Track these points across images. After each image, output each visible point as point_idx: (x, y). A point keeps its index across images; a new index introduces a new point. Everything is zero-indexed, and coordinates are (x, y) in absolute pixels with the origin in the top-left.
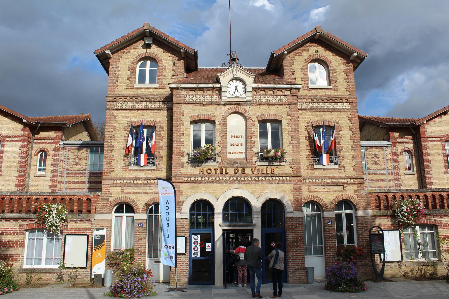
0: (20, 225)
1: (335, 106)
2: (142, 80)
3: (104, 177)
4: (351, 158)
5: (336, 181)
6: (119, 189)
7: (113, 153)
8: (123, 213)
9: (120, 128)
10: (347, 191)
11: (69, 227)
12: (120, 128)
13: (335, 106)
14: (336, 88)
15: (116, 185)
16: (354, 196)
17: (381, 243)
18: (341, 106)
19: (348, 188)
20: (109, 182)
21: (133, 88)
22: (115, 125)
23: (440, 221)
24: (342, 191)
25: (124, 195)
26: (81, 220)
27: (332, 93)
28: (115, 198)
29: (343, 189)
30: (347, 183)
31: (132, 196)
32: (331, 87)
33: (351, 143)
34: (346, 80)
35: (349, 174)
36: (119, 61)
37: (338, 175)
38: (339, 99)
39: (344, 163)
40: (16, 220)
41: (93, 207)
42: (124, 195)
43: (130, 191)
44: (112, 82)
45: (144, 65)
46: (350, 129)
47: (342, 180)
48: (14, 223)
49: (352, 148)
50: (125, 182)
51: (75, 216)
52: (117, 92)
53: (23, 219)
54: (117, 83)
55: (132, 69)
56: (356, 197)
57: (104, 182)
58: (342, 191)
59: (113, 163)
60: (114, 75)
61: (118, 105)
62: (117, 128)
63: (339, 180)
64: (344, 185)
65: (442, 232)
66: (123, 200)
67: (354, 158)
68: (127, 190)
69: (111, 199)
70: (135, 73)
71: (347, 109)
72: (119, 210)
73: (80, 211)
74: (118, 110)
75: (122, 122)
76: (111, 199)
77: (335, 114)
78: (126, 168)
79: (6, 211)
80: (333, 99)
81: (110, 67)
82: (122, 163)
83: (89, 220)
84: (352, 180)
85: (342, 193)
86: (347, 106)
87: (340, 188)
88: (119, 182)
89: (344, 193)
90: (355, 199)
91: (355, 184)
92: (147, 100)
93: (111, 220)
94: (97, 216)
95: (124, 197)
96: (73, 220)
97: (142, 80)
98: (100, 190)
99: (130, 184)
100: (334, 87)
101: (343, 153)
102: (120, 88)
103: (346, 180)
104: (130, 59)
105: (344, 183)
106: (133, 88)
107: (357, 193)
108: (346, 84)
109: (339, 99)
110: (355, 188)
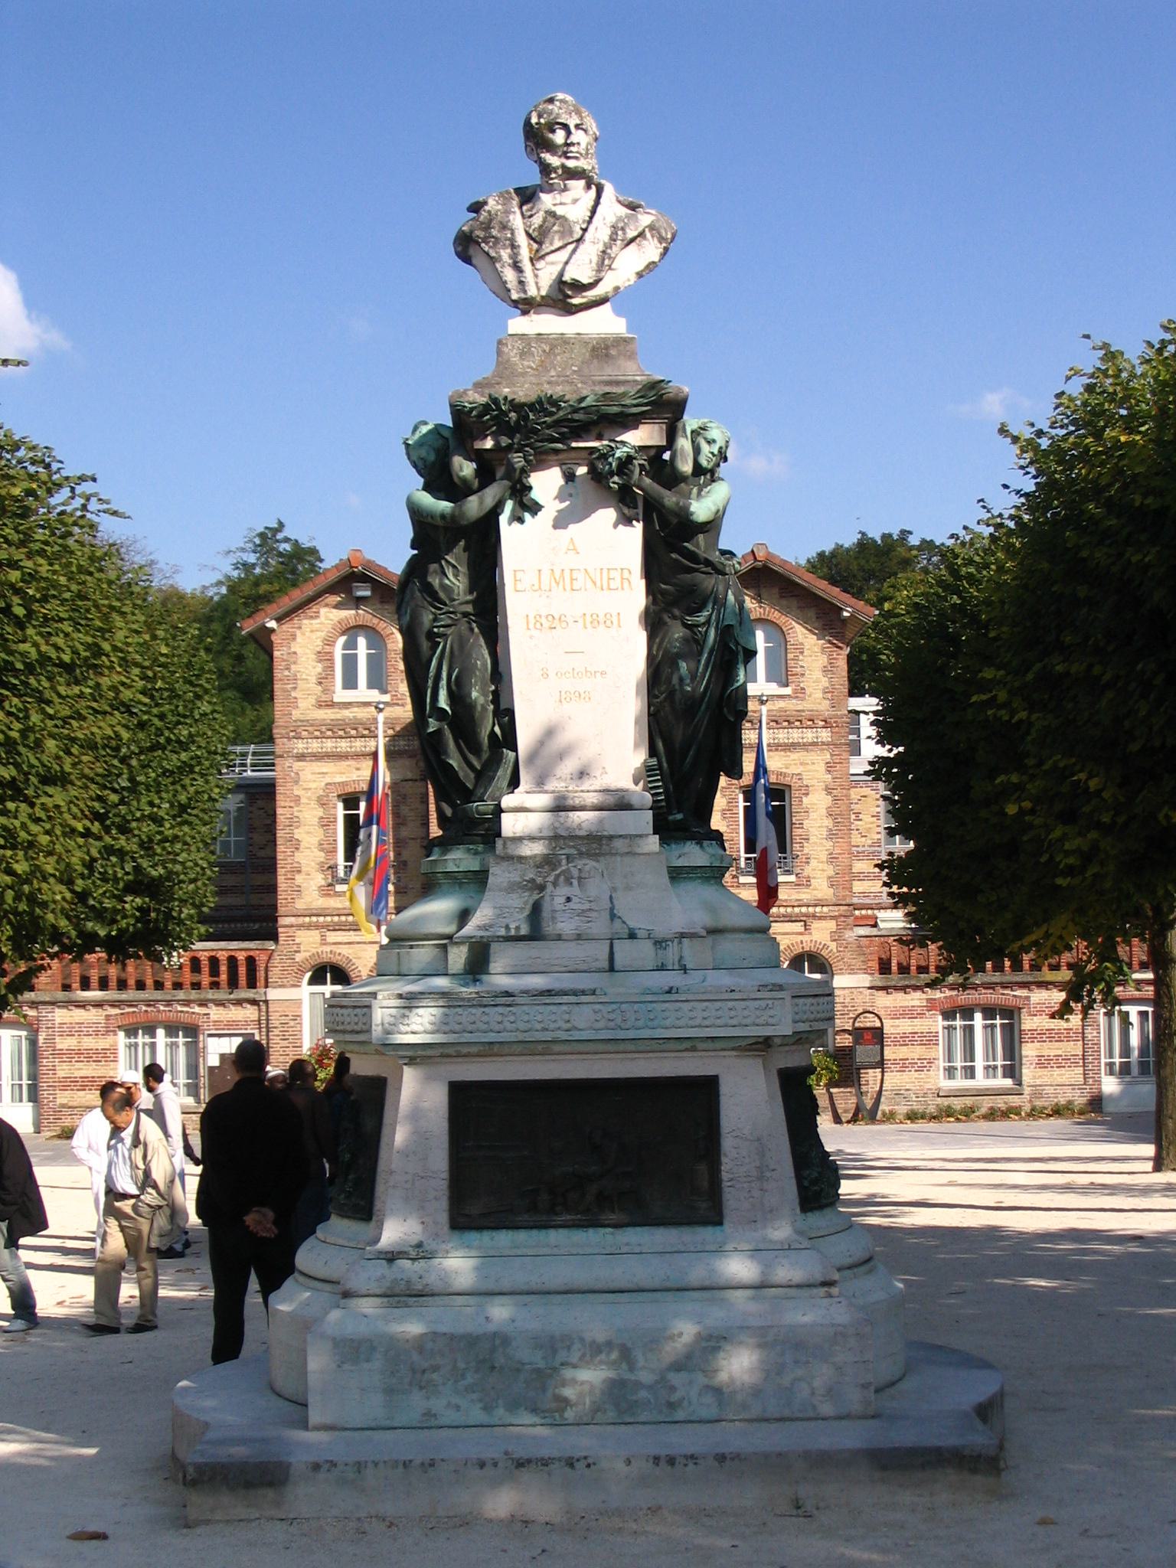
0: (108, 1017)
1: (795, 735)
2: (350, 683)
3: (281, 910)
4: (824, 857)
5: (789, 910)
6: (314, 936)
7: (299, 857)
8: (325, 983)
9: (309, 798)
10: (813, 932)
11: (213, 1017)
12: (309, 798)
13: (795, 735)
14: (800, 693)
15: (309, 927)
16: (829, 943)
17: (878, 1047)
18: (809, 735)
19: (815, 925)
20: (292, 920)
21: (332, 705)
22: (296, 793)
23: (1028, 998)
24: (801, 934)
25: (328, 949)
26: (239, 1003)
27: (791, 705)
28: (308, 954)
29: (802, 929)
30: (814, 916)
31: (345, 950)
32: (788, 691)
33: (828, 823)
34: (825, 671)
35: (820, 896)
36: (294, 637)
37: (793, 897)
38: (808, 721)
39: (808, 871)
40: (99, 1005)
41: (261, 974)
42: (328, 949)
43: (339, 939)
44: (285, 691)
45: (351, 645)
46: (828, 790)
47: (804, 910)
48: (93, 1011)
49: (831, 835)
50: (329, 919)
51: (221, 995)
52: (296, 714)
53: (114, 1004)
54: (293, 694)
55: (325, 658)
56: (833, 946)
57: (282, 921)
58: (801, 934)
59: (299, 879)
60: (286, 673)
61: (300, 746)
62: (303, 800)
63: (797, 910)
64: (805, 920)
65: (1028, 1023)
66: (326, 958)
67: (832, 859)
68: (332, 937)
69: (298, 957)
70: (332, 668)
71: (823, 743)
72: (318, 978)
73: (233, 983)
74: (301, 757)
75: (313, 785)
76: (298, 957)
77: (794, 756)
78: (328, 889)
79: (74, 986)
80: (792, 719)
81: (276, 654)
82: (320, 879)
83: (254, 1002)
84: (825, 909)
85: (800, 938)
86: (825, 735)
87: (798, 927)
88: (314, 919)
89: (805, 938)
90: (831, 950)
91: (833, 918)
92: (366, 732)
93: (298, 1002)
94: (273, 994)
95: (327, 953)
96: (220, 1003)
97: (350, 683)
98: (274, 937)
99: (339, 924)
100: (795, 691)
101: (807, 849)
102: (302, 704)
103: (811, 909)
104: (319, 634)
105: (807, 915)
106: (332, 705)
107: (836, 936)
108: (825, 682)
109: (808, 721)
110: (832, 925)
